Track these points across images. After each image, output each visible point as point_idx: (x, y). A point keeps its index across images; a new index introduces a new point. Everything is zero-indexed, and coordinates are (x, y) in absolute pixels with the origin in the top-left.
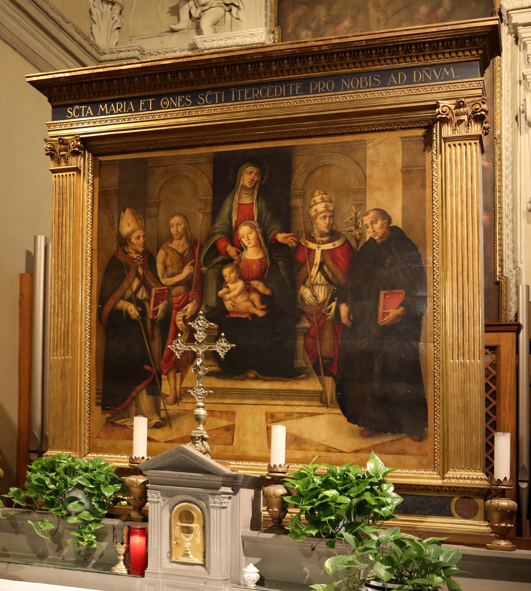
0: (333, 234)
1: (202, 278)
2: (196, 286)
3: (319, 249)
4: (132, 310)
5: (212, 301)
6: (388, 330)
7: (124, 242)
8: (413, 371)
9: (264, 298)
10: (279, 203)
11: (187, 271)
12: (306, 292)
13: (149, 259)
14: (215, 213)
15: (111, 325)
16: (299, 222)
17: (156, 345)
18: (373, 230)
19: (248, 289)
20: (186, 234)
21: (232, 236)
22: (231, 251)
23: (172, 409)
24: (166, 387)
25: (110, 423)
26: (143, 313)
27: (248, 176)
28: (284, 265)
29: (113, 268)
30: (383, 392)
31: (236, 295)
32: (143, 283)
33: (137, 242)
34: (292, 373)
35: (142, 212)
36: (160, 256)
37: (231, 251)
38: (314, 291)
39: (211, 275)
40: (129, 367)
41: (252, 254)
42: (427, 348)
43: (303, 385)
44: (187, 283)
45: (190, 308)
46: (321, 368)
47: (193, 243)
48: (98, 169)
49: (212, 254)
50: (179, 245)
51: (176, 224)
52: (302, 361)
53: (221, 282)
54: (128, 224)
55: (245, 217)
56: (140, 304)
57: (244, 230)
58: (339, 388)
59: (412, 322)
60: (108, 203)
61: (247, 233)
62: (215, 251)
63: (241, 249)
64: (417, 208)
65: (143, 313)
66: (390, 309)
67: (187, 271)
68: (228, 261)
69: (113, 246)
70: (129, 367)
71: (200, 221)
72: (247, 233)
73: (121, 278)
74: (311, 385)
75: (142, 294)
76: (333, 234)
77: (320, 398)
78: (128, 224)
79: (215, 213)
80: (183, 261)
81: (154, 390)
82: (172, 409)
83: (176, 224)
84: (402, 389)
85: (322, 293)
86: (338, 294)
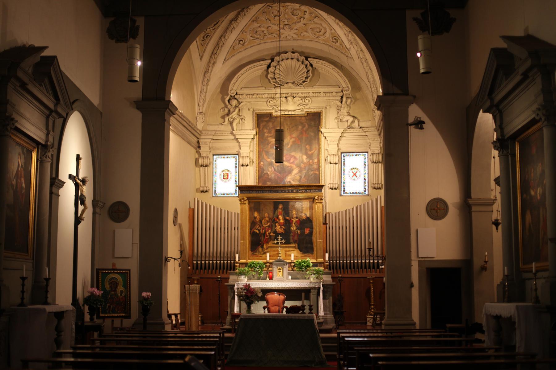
0: (297, 218)
1: (272, 225)
2: (271, 227)
3: (294, 220)
4: (257, 231)
5: (274, 230)
6: (307, 235)
7: (255, 218)
8: (311, 242)
9: (284, 229)
10: (286, 212)
11: (269, 224)
12: (292, 228)
13: (261, 222)
14: (274, 213)
15: (253, 234)
16: (291, 215)
17: (263, 238)
18: (304, 217)
19: (281, 228)
20: (268, 217)
21: (278, 218)
22: (278, 220)
23: (266, 251)
24: (265, 246)
25: (253, 254)
26: (260, 232)
27: (281, 206)
28: (288, 223)
29: (253, 223)
30: (306, 246)
31: (278, 228)
32: (260, 226)
33: (258, 218)
34: (290, 243)
35: (259, 211)
36: (263, 221)
37: (278, 220)
38: (293, 228)
39: (274, 225)
40: (257, 242)
41: (282, 221)
42: (314, 238)
43: (291, 245)
44: (269, 226)
45: (269, 231)
46: (295, 242)
47: (270, 219)
48: (249, 203)
49: (274, 221)
50: (267, 219)
51: (266, 215)
52: (291, 241)
53: (276, 226)
54: (256, 214)
55: (280, 214)
56: (259, 230)
57: (280, 216)
58: (298, 246)
59: (311, 233)
60: (252, 210)
61: (281, 217)
62: (274, 220)
63: (279, 220)
64: (312, 214)
65: (260, 232)
66: (307, 231)
67: (269, 224)
68: (277, 222)
69: (253, 219)
70: (257, 242)
71: (271, 215)
72: (281, 217)
73: (255, 225)
74: (293, 245)
75: (259, 228)
76: (297, 218)
77: (295, 247)
78: (256, 214)
79: (274, 213)
80: (268, 222)
81: (262, 247)
82: (266, 251)
83: (266, 215)
84: (309, 245)
85: (295, 228)
86: (298, 229)
